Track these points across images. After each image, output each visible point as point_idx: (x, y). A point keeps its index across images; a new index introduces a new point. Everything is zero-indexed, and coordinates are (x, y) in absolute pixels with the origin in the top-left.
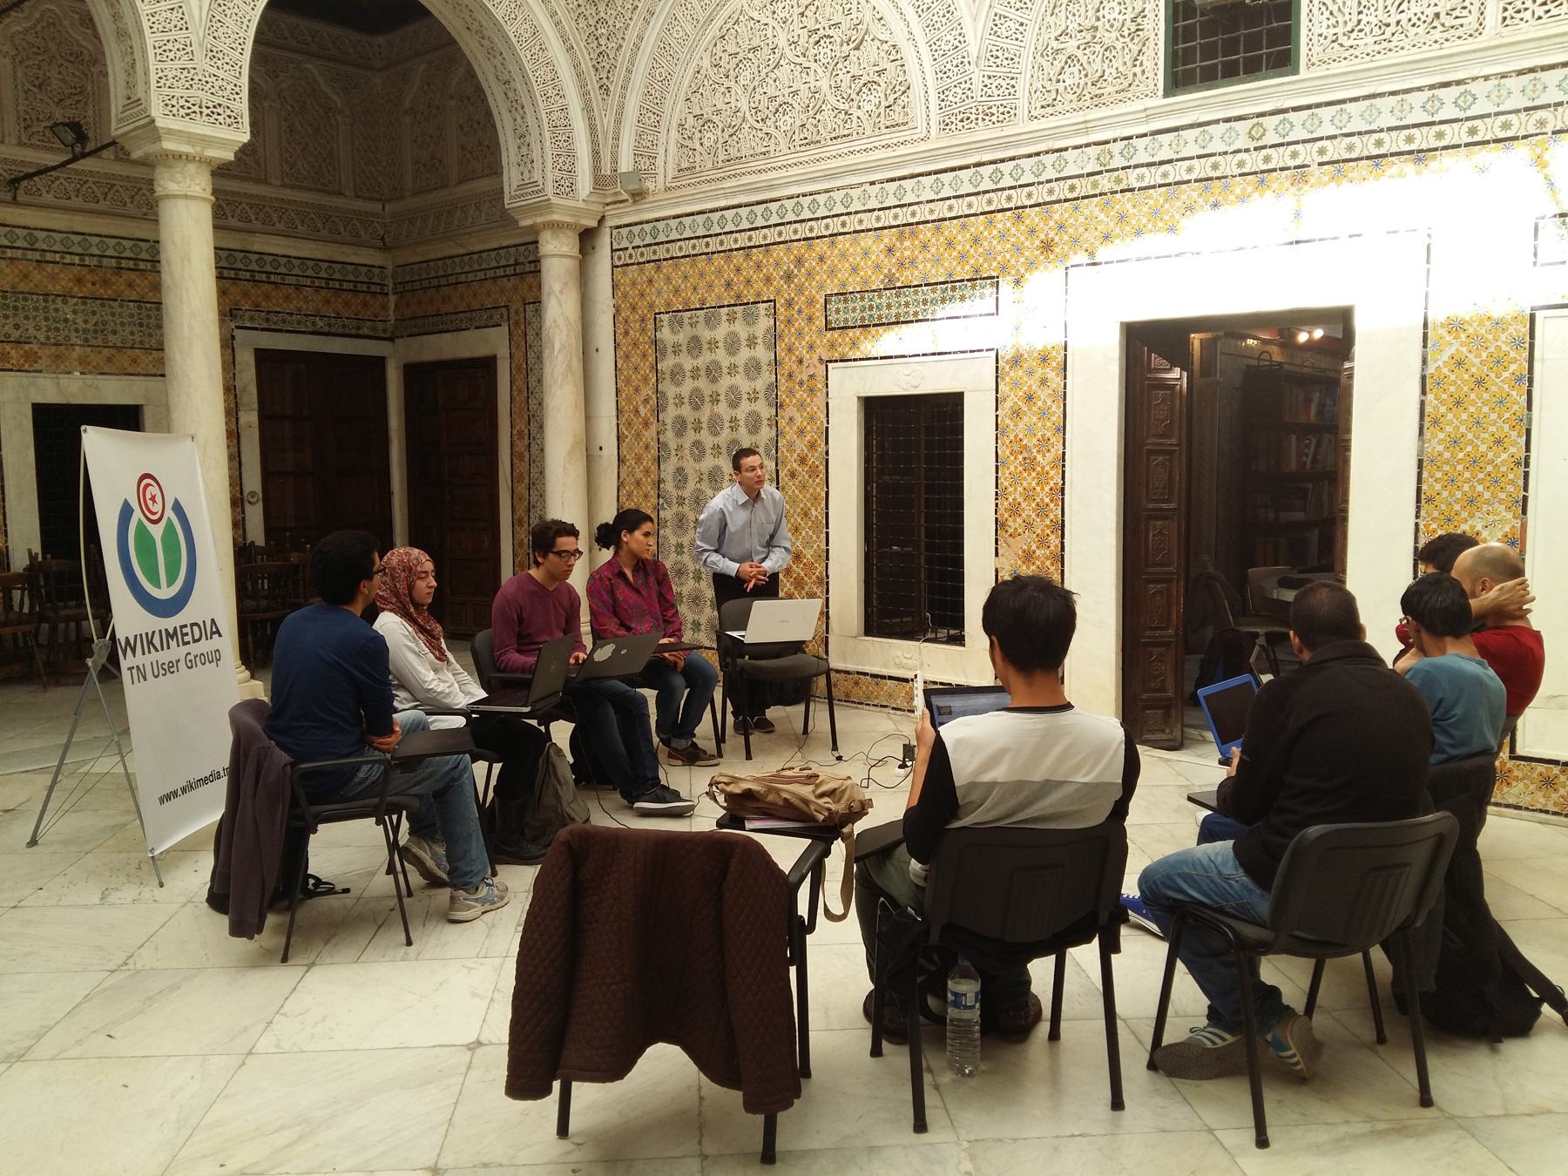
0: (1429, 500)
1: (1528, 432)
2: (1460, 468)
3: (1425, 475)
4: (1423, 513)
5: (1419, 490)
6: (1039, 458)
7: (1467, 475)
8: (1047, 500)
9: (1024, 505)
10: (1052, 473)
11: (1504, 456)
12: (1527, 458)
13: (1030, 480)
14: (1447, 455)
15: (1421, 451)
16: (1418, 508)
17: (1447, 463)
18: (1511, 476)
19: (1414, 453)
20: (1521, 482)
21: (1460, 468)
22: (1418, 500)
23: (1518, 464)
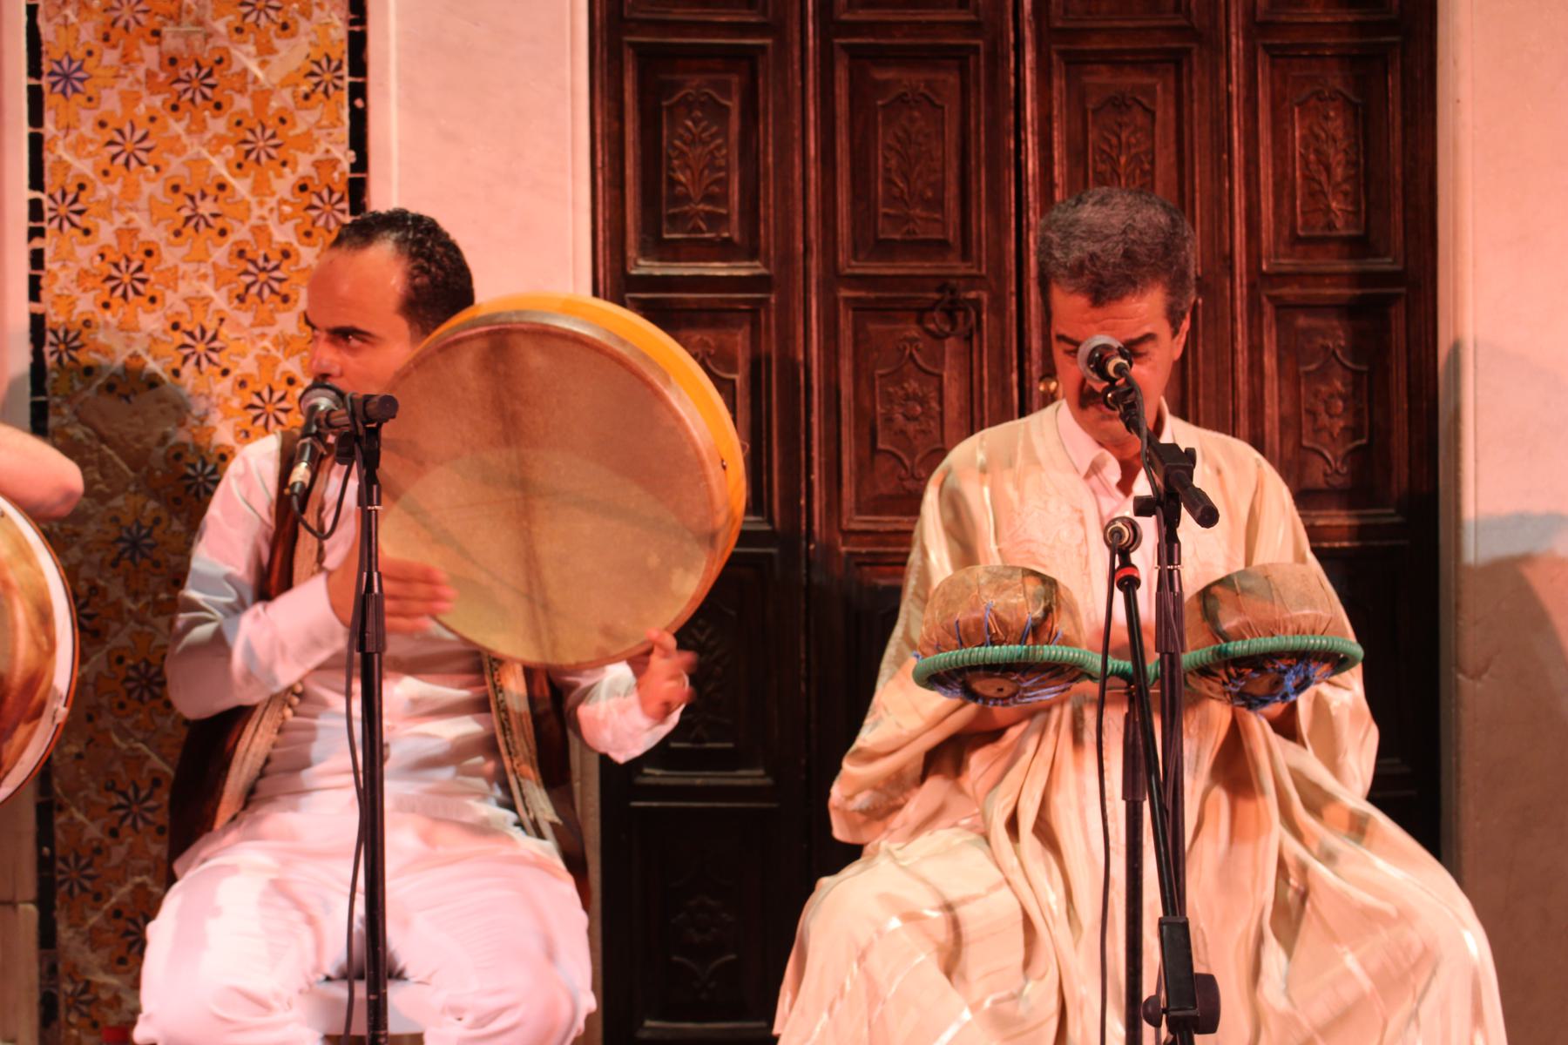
6: (245, 57)
8: (283, 235)
9: (171, 256)
10: (305, 120)
13: (202, 150)
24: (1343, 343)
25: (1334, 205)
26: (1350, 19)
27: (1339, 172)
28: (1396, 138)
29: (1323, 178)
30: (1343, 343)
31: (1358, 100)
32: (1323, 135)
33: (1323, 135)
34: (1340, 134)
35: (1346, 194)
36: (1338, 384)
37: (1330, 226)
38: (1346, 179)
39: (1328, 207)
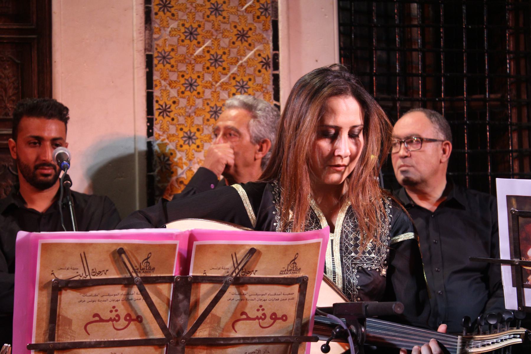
0: (165, 111)
1: (275, 24)
2: (199, 68)
3: (156, 77)
4: (156, 129)
5: (150, 98)
7: (208, 78)
11: (250, 54)
12: (276, 57)
14: (182, 50)
15: (149, 46)
16: (150, 122)
17: (182, 61)
18: (259, 80)
19: (139, 45)
20: (270, 88)
21: (199, 68)
22: (150, 111)
23: (266, 64)
24: (12, 164)
25: (8, 105)
26: (15, 27)
27: (11, 92)
28: (35, 79)
29: (4, 94)
30: (12, 164)
31: (19, 62)
32: (3, 76)
33: (3, 76)
34: (10, 74)
35: (13, 101)
36: (10, 182)
37: (7, 114)
38: (13, 95)
39: (6, 107)
